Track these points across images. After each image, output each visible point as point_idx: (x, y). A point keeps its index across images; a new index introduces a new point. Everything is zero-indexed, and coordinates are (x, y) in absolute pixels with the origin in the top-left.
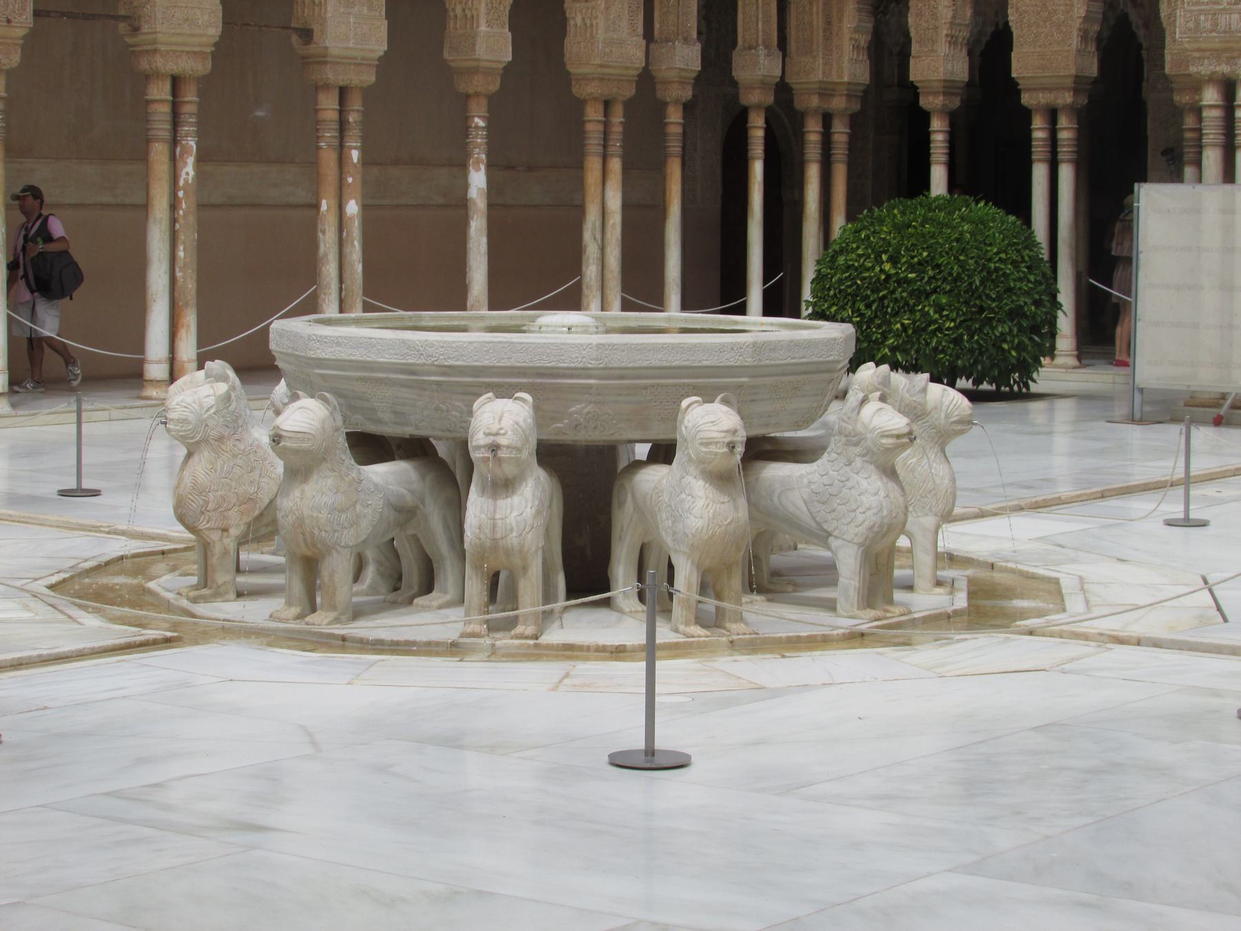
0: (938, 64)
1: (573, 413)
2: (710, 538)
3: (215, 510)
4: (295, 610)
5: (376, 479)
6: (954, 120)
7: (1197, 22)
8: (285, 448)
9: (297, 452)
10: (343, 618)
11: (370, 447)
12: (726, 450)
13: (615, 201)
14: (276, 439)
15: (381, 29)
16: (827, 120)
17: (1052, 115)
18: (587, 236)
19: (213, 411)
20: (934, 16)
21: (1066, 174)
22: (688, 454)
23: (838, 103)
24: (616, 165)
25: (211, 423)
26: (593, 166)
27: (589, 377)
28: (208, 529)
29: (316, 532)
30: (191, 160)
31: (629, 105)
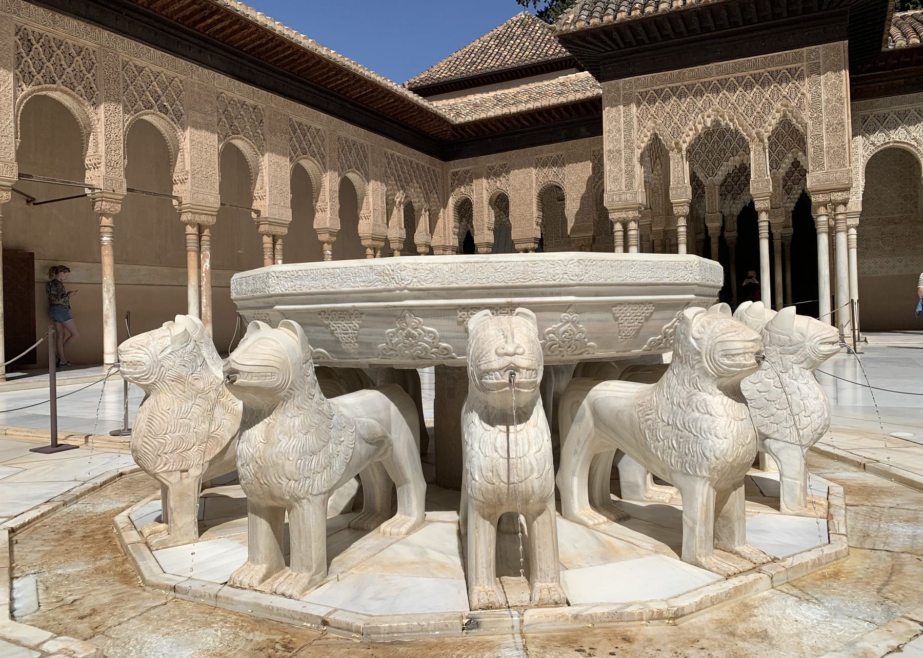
1: (549, 333)
2: (735, 460)
4: (262, 568)
5: (345, 411)
8: (238, 386)
9: (257, 389)
10: (318, 578)
11: (336, 379)
12: (753, 361)
14: (231, 376)
15: (289, 212)
19: (169, 350)
20: (482, 220)
22: (703, 368)
25: (167, 363)
28: (165, 472)
29: (284, 482)
30: (208, 261)
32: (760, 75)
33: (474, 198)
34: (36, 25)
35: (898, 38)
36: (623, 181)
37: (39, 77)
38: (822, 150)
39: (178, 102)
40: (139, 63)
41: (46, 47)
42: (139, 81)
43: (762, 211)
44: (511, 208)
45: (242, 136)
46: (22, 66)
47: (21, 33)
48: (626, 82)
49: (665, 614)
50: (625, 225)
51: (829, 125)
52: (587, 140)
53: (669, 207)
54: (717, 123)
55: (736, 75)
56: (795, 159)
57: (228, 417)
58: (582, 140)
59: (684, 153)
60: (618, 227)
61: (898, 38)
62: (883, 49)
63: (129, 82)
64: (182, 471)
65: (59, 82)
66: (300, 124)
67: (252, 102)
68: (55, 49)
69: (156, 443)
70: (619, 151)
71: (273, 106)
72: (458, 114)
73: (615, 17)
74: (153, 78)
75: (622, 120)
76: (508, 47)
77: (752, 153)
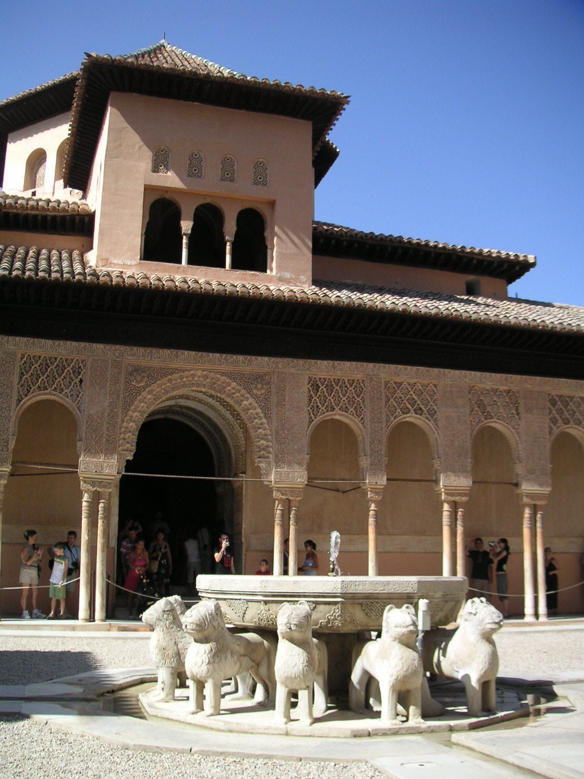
34: (322, 373)
37: (323, 408)
39: (431, 403)
40: (398, 380)
41: (330, 388)
42: (399, 394)
45: (495, 420)
46: (312, 404)
47: (312, 382)
63: (390, 396)
65: (337, 409)
66: (561, 397)
67: (506, 388)
68: (335, 386)
71: (529, 386)
74: (410, 389)
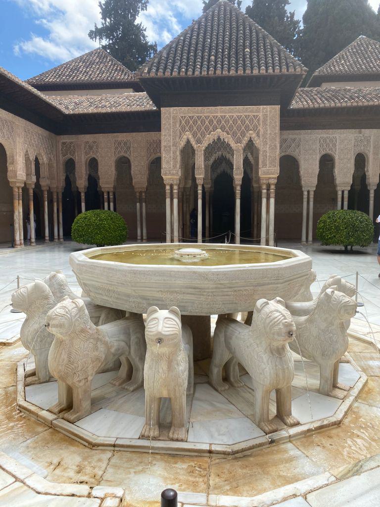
0: (82, 183)
3: (81, 370)
6: (86, 193)
7: (166, 172)
13: (21, 210)
16: (57, 193)
17: (108, 193)
18: (15, 218)
19: (78, 316)
20: (82, 173)
21: (112, 204)
23: (61, 190)
24: (21, 202)
26: (16, 202)
27: (277, 284)
31: (23, 188)
32: (241, 116)
33: (76, 159)
35: (295, 104)
36: (172, 163)
38: (266, 157)
43: (238, 185)
44: (100, 168)
48: (174, 110)
49: (337, 423)
50: (171, 186)
51: (270, 146)
52: (144, 133)
53: (194, 179)
54: (219, 139)
55: (230, 114)
56: (247, 155)
57: (102, 346)
58: (141, 133)
59: (203, 152)
60: (168, 187)
61: (295, 104)
62: (288, 108)
64: (85, 379)
69: (73, 367)
70: (170, 147)
72: (67, 108)
73: (171, 74)
75: (172, 130)
76: (92, 69)
77: (235, 155)
